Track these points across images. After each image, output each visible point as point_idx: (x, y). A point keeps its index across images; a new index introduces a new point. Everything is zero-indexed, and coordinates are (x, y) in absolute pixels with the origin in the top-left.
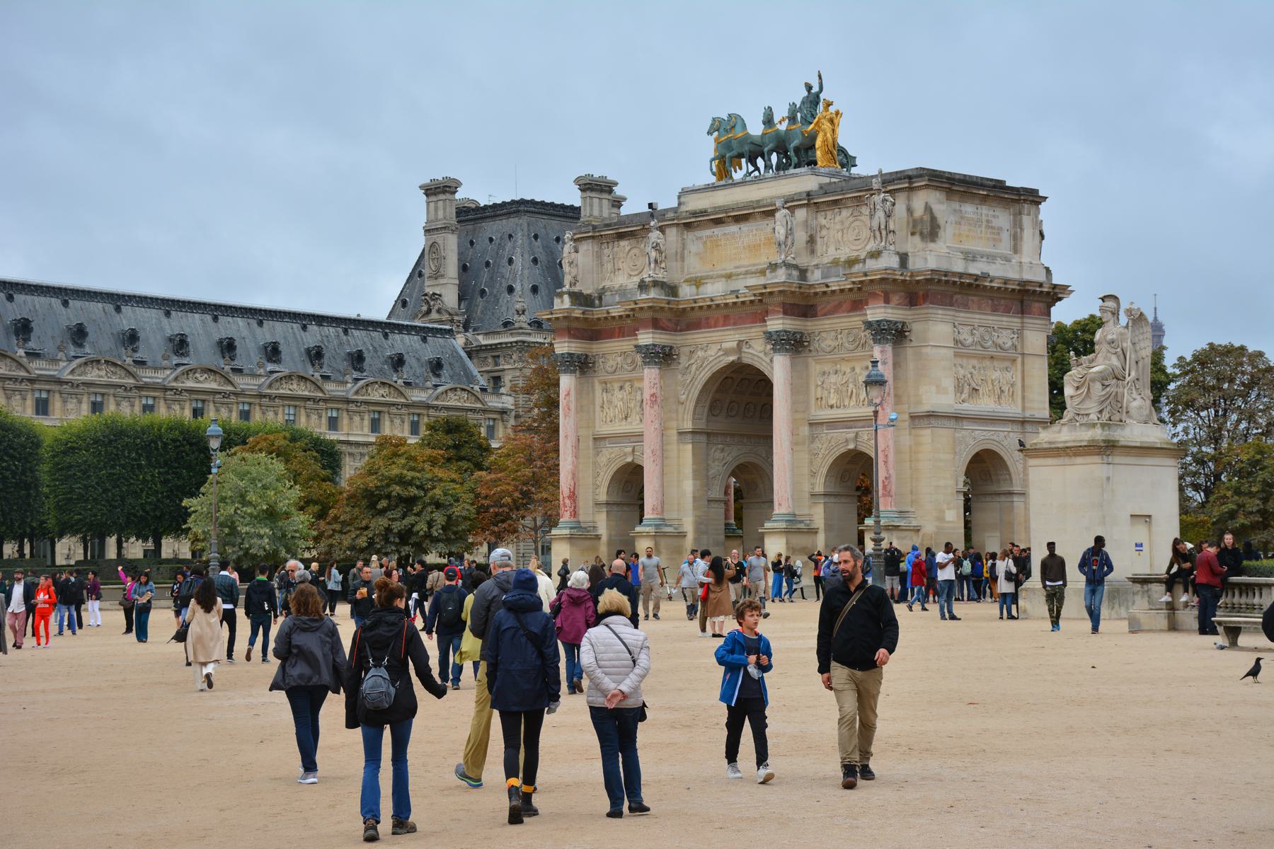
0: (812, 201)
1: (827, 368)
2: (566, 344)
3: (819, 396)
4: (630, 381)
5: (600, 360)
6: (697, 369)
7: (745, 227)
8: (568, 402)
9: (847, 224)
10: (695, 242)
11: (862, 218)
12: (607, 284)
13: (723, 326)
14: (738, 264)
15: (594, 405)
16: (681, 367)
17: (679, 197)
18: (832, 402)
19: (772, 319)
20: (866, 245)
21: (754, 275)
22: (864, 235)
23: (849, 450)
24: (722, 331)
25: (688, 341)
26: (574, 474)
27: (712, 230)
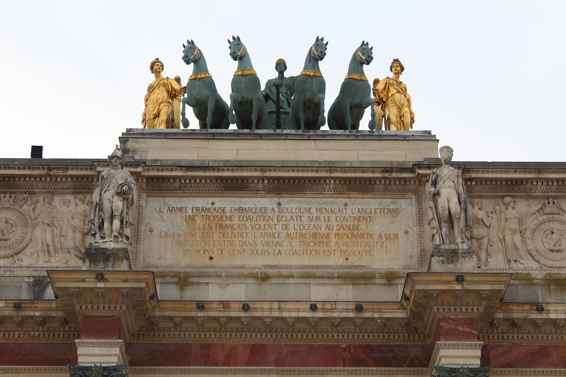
0: (467, 175)
9: (531, 223)
14: (274, 262)
17: (124, 139)
19: (449, 347)
21: (327, 281)
27: (211, 200)
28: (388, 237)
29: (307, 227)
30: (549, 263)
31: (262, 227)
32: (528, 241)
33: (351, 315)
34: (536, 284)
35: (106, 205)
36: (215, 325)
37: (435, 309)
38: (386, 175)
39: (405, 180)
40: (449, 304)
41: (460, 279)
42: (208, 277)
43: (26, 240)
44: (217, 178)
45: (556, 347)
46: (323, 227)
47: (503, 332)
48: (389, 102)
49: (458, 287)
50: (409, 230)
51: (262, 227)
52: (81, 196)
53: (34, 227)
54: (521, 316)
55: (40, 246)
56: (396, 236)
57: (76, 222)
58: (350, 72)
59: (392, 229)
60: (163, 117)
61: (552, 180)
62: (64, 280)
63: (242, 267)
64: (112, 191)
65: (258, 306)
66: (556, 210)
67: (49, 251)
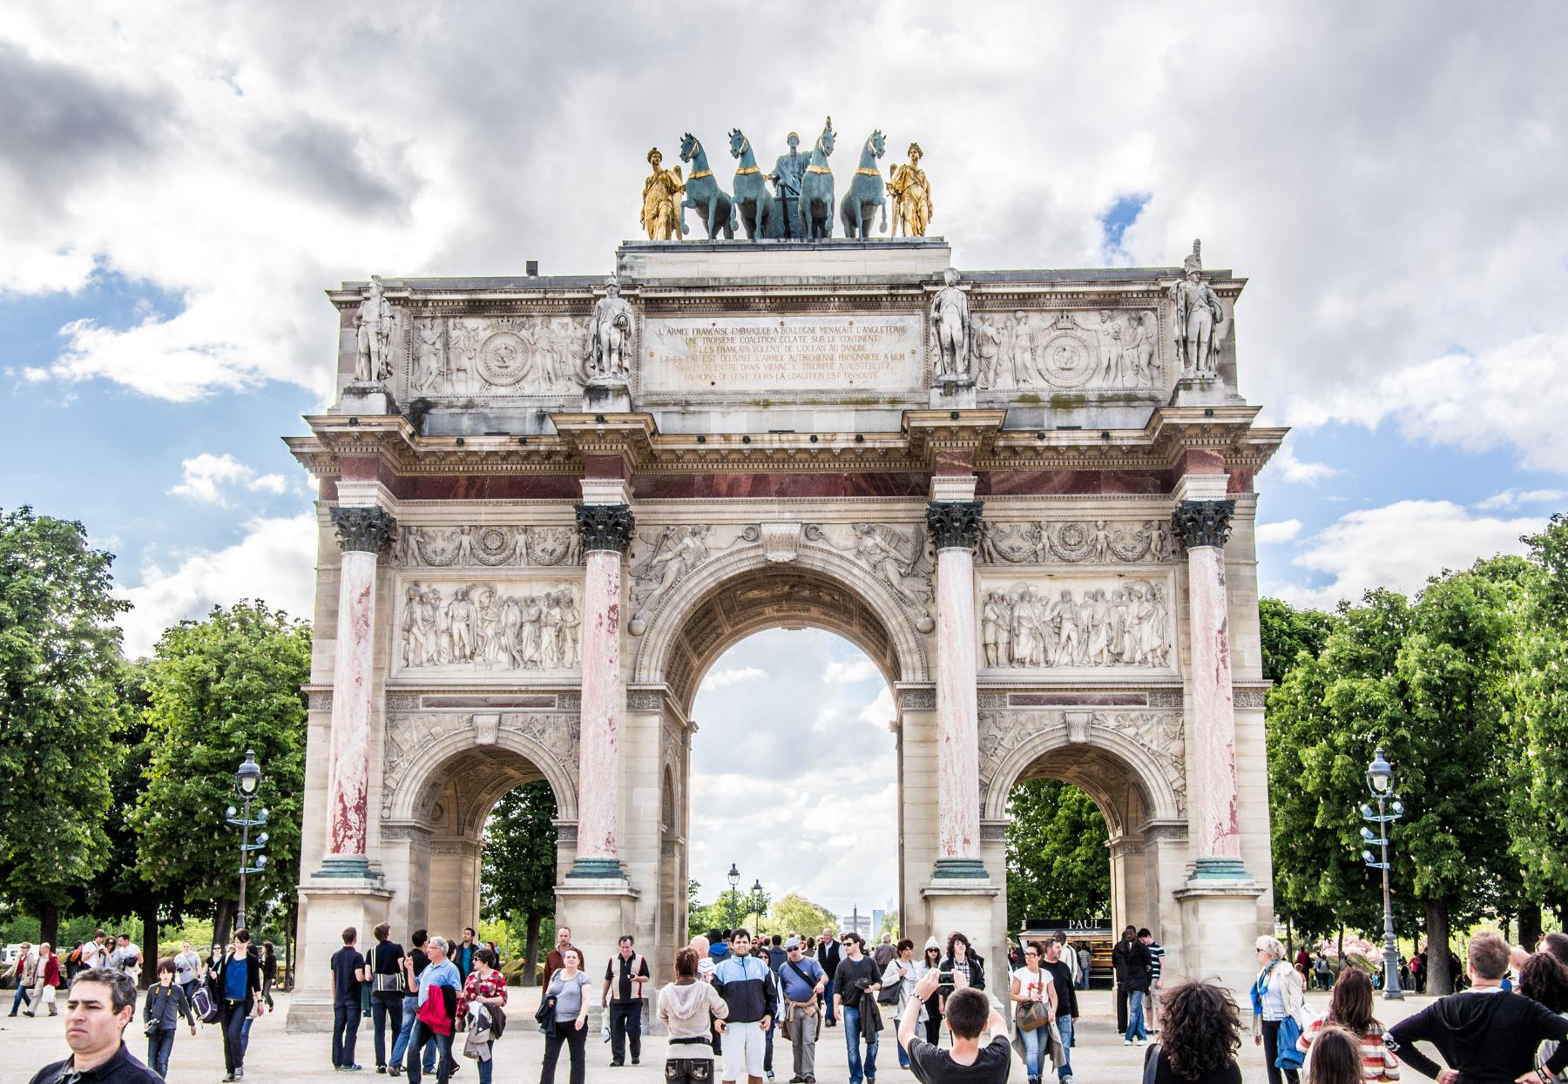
0: (977, 290)
1: (1002, 585)
2: (375, 491)
3: (990, 639)
4: (485, 584)
6: (679, 570)
7: (794, 321)
8: (366, 609)
10: (660, 335)
11: (1079, 333)
12: (428, 393)
13: (751, 494)
15: (392, 626)
16: (632, 563)
17: (621, 255)
21: (829, 408)
22: (1083, 364)
23: (1074, 744)
24: (755, 502)
25: (661, 516)
26: (367, 761)
27: (712, 320)
30: (1059, 382)
32: (1039, 360)
33: (852, 445)
34: (1043, 408)
35: (604, 338)
36: (716, 456)
37: (931, 444)
38: (894, 292)
40: (945, 439)
41: (955, 415)
42: (709, 404)
43: (527, 367)
44: (717, 298)
45: (1058, 473)
48: (905, 194)
49: (954, 423)
52: (579, 319)
53: (534, 353)
54: (1023, 443)
56: (902, 356)
58: (862, 166)
59: (898, 350)
60: (662, 219)
61: (1067, 293)
62: (565, 423)
63: (743, 393)
65: (759, 438)
66: (1070, 326)
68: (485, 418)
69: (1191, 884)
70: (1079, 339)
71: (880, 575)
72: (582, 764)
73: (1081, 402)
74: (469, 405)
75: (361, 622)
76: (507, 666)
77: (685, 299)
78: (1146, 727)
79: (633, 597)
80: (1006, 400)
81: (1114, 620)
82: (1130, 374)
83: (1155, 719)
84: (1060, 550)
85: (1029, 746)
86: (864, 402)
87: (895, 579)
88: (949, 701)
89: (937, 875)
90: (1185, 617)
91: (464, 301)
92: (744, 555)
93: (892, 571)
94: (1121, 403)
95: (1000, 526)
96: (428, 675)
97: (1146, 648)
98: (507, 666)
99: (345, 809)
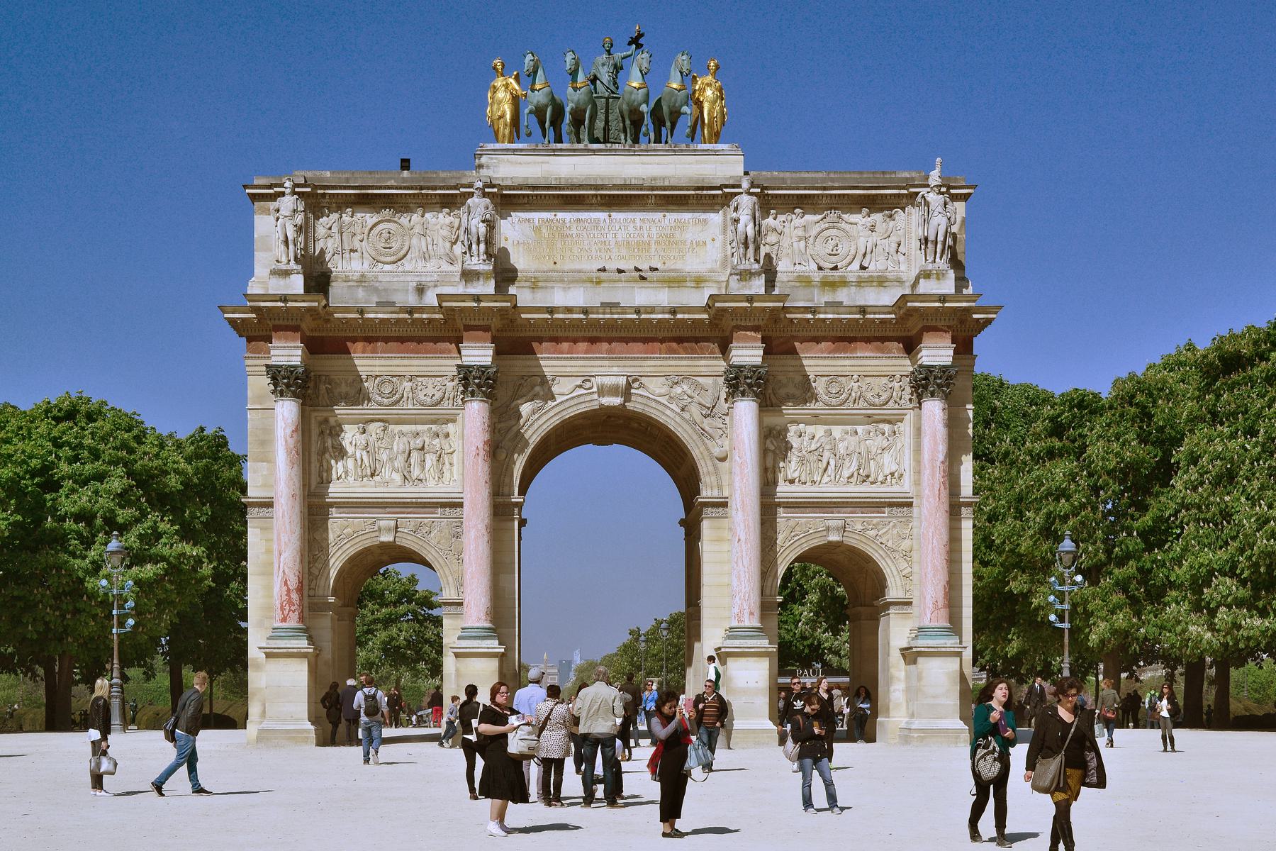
3: (769, 463)
5: (323, 388)
6: (534, 412)
7: (619, 216)
9: (813, 232)
11: (843, 225)
13: (586, 353)
18: (796, 475)
20: (850, 264)
28: (698, 244)
29: (632, 236)
31: (596, 235)
33: (667, 316)
35: (474, 230)
39: (714, 196)
44: (558, 195)
46: (646, 236)
47: (784, 327)
50: (716, 238)
51: (596, 235)
55: (417, 254)
56: (705, 243)
57: (445, 232)
63: (579, 271)
64: (479, 218)
66: (836, 220)
67: (425, 257)
68: (376, 290)
69: (913, 644)
70: (843, 230)
71: (686, 415)
72: (465, 556)
73: (844, 283)
74: (362, 280)
75: (294, 452)
76: (400, 483)
77: (532, 195)
78: (885, 530)
79: (496, 431)
80: (786, 280)
81: (863, 450)
82: (882, 259)
83: (891, 524)
84: (825, 398)
85: (797, 544)
86: (676, 281)
87: (698, 418)
88: (740, 513)
89: (729, 637)
90: (918, 449)
91: (355, 195)
92: (582, 399)
93: (695, 411)
94: (875, 284)
95: (780, 378)
96: (340, 490)
97: (887, 472)
98: (400, 483)
99: (288, 590)
